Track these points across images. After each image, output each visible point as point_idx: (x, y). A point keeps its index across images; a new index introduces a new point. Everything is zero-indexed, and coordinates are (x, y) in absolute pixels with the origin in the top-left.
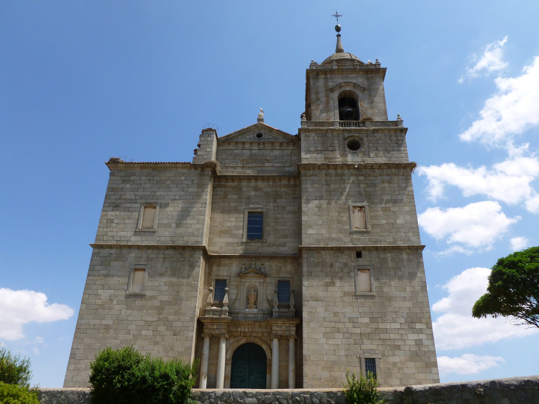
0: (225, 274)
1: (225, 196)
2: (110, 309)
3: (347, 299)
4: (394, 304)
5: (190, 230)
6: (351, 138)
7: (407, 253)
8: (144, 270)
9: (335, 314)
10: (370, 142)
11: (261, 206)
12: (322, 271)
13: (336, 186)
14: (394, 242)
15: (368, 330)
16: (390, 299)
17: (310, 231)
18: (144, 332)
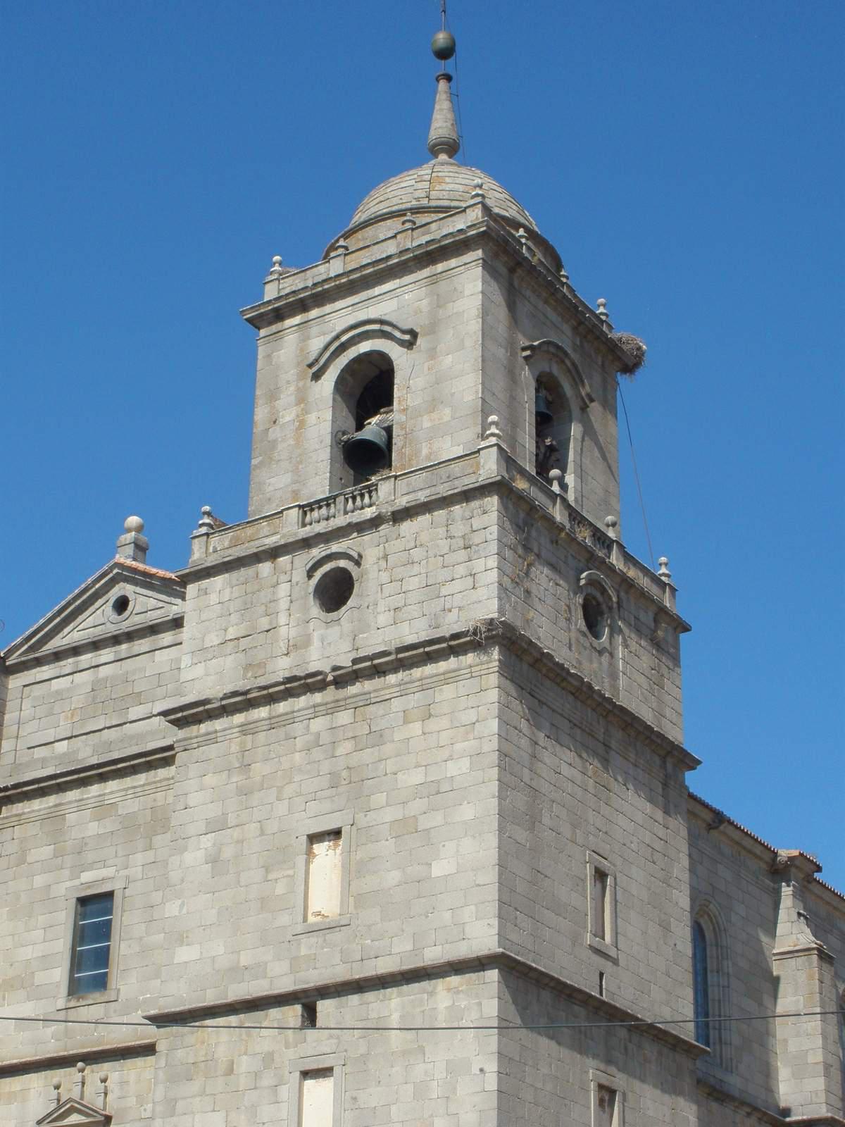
1: (22, 861)
7: (449, 990)
10: (383, 563)
12: (203, 1093)
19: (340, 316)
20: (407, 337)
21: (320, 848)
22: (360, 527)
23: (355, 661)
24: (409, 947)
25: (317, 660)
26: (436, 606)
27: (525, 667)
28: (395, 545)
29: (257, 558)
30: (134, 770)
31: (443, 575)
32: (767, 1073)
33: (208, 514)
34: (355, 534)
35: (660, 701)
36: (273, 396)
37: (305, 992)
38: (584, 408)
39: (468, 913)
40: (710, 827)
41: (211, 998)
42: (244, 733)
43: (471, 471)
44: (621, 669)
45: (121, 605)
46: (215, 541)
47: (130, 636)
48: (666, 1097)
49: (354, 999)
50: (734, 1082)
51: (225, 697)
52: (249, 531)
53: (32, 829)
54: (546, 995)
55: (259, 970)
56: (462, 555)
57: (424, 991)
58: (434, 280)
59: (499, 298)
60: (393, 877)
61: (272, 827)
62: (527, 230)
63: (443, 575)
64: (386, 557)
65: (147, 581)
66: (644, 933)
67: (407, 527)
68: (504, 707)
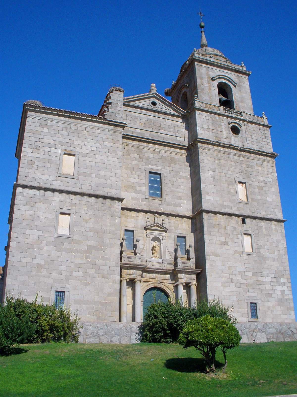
0: (133, 225)
2: (40, 249)
3: (237, 256)
5: (109, 182)
8: (69, 214)
9: (229, 268)
13: (225, 162)
15: (252, 282)
17: (208, 197)
18: (74, 273)
30: (164, 145)
39: (276, 210)
45: (154, 104)
49: (254, 221)
57: (269, 223)
61: (228, 176)
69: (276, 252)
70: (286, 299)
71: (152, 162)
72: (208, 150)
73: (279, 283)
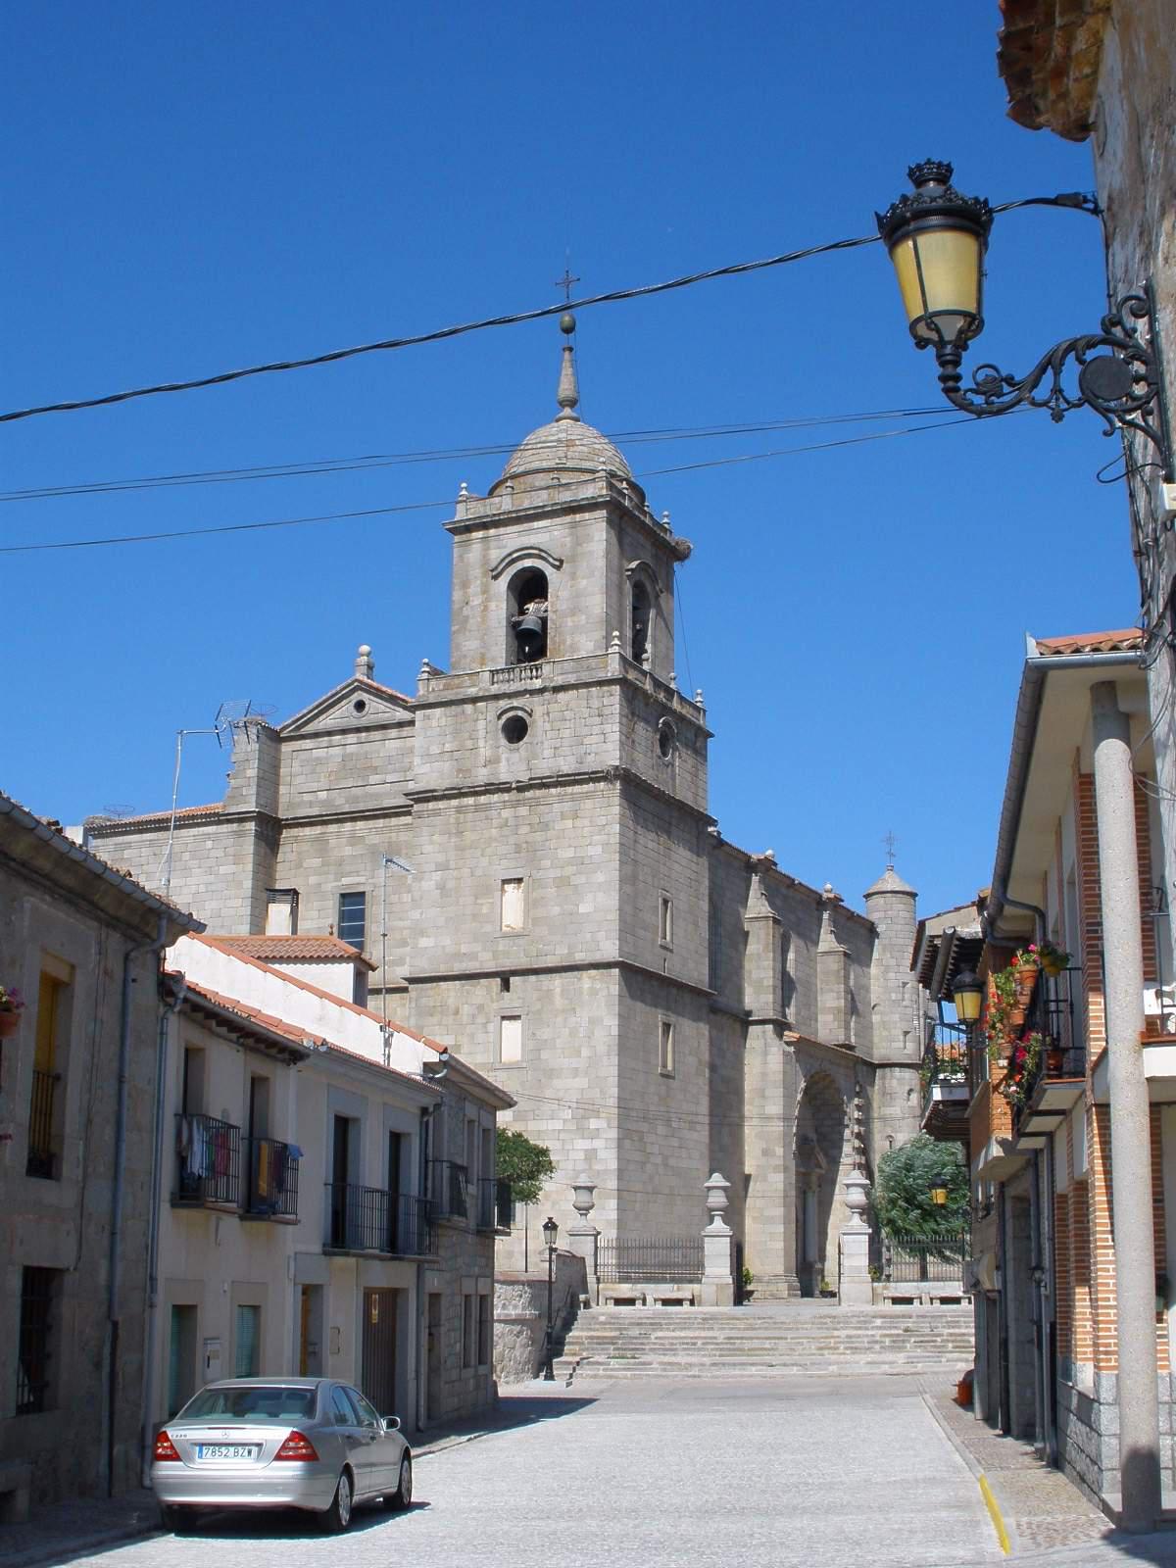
1: (299, 866)
4: (557, 1083)
6: (511, 714)
7: (589, 978)
10: (546, 717)
11: (362, 879)
14: (570, 954)
16: (551, 1073)
19: (512, 538)
20: (557, 563)
21: (509, 888)
22: (532, 692)
23: (531, 779)
24: (566, 951)
25: (504, 774)
26: (582, 750)
27: (632, 788)
28: (554, 707)
29: (463, 701)
31: (585, 731)
32: (739, 992)
33: (427, 664)
34: (528, 696)
35: (697, 787)
36: (465, 585)
37: (504, 972)
38: (657, 597)
40: (714, 848)
41: (443, 971)
42: (459, 812)
43: (602, 666)
44: (677, 778)
45: (360, 706)
46: (433, 683)
47: (367, 729)
48: (695, 1024)
49: (533, 978)
50: (722, 1001)
51: (447, 789)
52: (456, 681)
53: (305, 847)
54: (640, 978)
55: (473, 956)
56: (598, 720)
58: (574, 525)
59: (614, 540)
60: (556, 910)
61: (479, 872)
62: (629, 483)
63: (585, 731)
64: (548, 713)
65: (378, 693)
66: (686, 931)
67: (561, 696)
68: (622, 816)
69: (585, 1052)
70: (598, 1171)
71: (348, 868)
72: (435, 815)
73: (582, 1131)
